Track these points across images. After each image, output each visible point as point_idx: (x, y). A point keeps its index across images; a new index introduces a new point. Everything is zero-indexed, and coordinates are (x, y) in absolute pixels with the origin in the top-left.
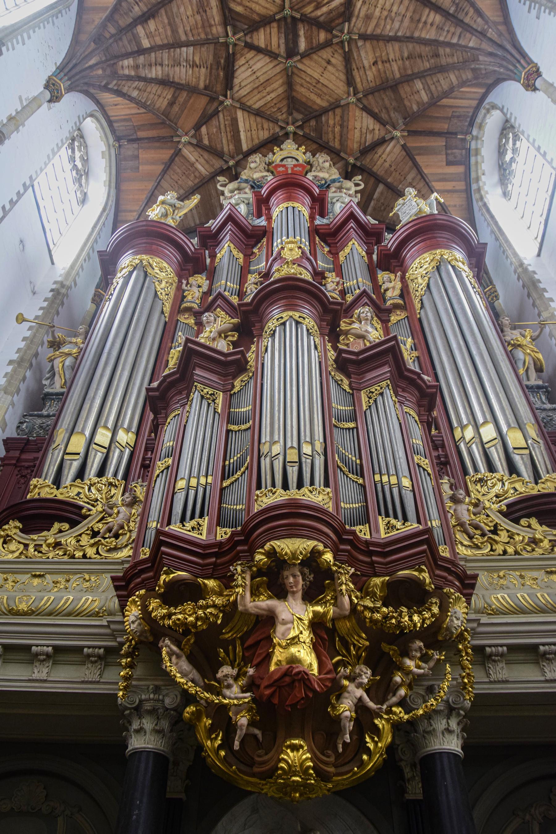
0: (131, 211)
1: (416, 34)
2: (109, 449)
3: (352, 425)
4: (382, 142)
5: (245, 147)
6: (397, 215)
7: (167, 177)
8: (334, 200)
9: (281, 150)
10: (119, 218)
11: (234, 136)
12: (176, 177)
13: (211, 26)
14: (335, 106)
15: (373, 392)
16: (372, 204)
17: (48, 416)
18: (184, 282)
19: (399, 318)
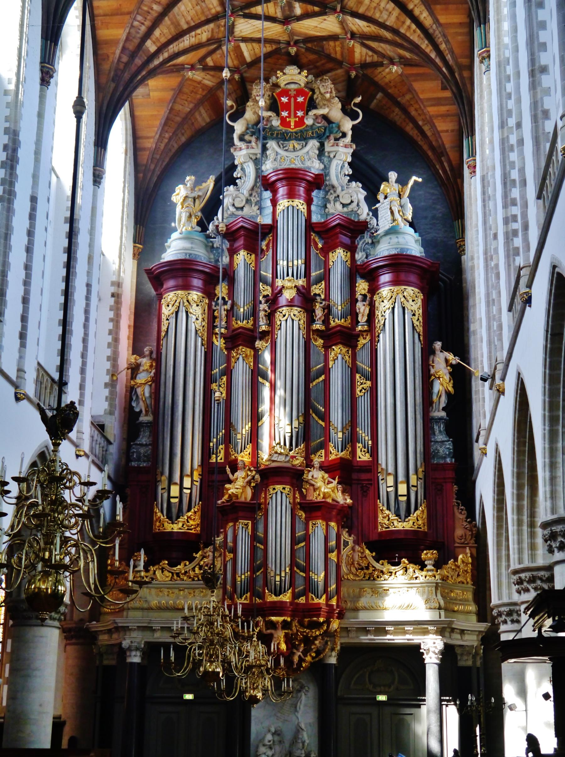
0: (148, 138)
1: (402, 31)
2: (191, 489)
4: (381, 64)
5: (248, 59)
6: (377, 209)
7: (178, 100)
8: (332, 155)
9: (284, 74)
10: (138, 146)
11: (237, 56)
12: (185, 97)
13: (209, 9)
14: (334, 37)
16: (375, 101)
17: (146, 445)
18: (214, 303)
19: (364, 341)
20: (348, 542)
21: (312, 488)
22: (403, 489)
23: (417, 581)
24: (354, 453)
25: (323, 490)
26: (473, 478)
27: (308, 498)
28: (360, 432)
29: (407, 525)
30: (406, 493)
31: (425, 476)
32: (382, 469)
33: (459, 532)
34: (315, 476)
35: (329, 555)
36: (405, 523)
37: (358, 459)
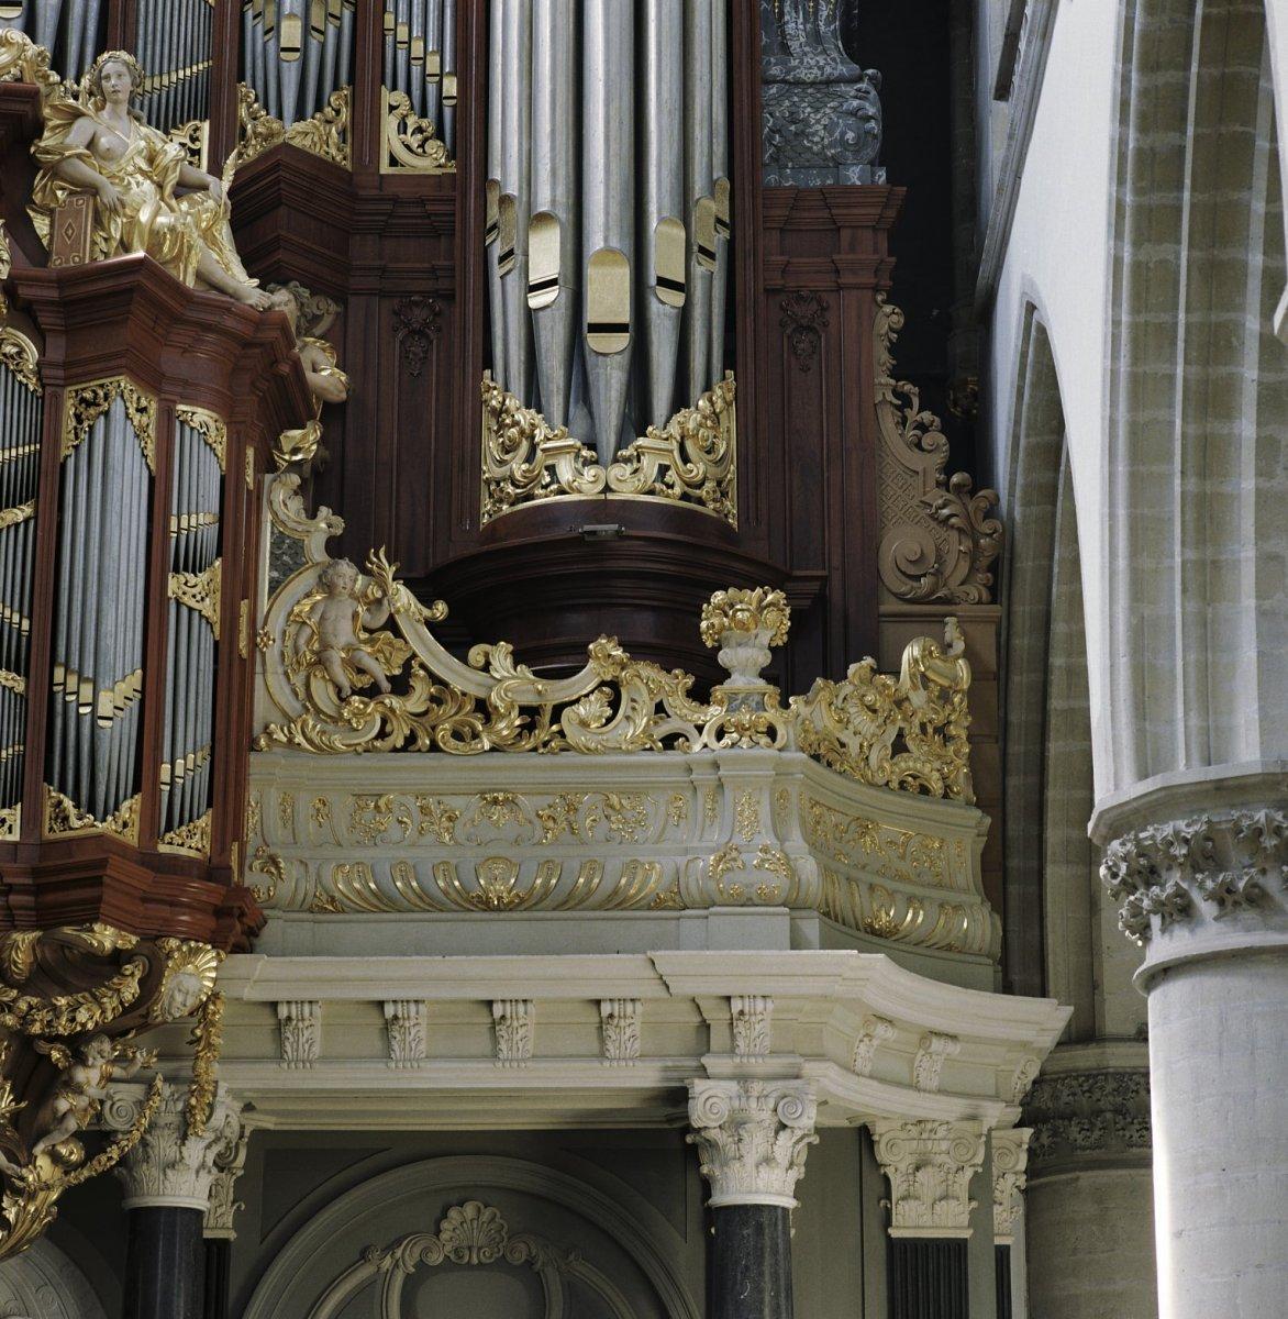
3: (26, 511)
15: (88, 404)
20: (297, 548)
21: (85, 205)
22: (609, 295)
23: (673, 757)
24: (363, 131)
25: (144, 216)
26: (984, 271)
27: (56, 262)
28: (402, 33)
29: (627, 484)
30: (625, 316)
31: (731, 245)
32: (505, 201)
33: (902, 542)
34: (104, 142)
35: (174, 584)
36: (620, 471)
37: (385, 169)
